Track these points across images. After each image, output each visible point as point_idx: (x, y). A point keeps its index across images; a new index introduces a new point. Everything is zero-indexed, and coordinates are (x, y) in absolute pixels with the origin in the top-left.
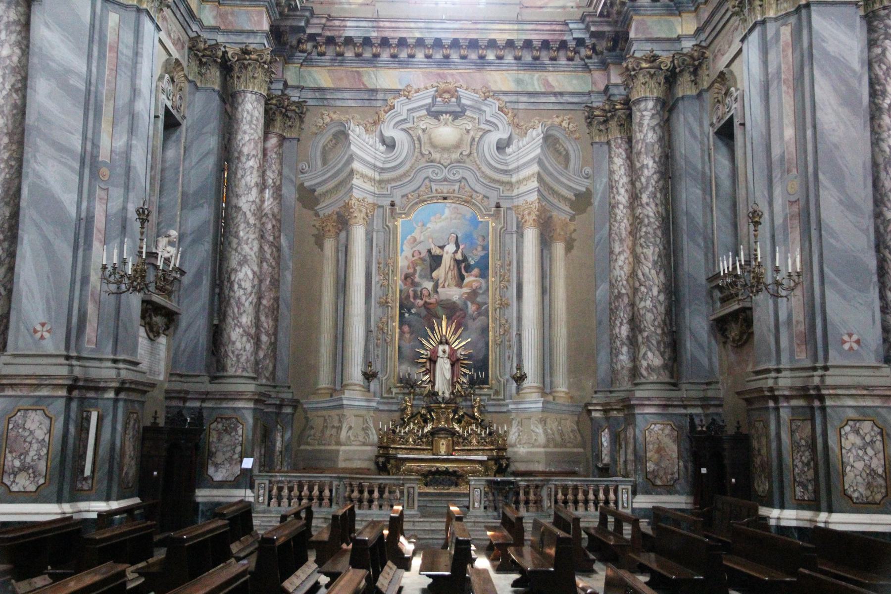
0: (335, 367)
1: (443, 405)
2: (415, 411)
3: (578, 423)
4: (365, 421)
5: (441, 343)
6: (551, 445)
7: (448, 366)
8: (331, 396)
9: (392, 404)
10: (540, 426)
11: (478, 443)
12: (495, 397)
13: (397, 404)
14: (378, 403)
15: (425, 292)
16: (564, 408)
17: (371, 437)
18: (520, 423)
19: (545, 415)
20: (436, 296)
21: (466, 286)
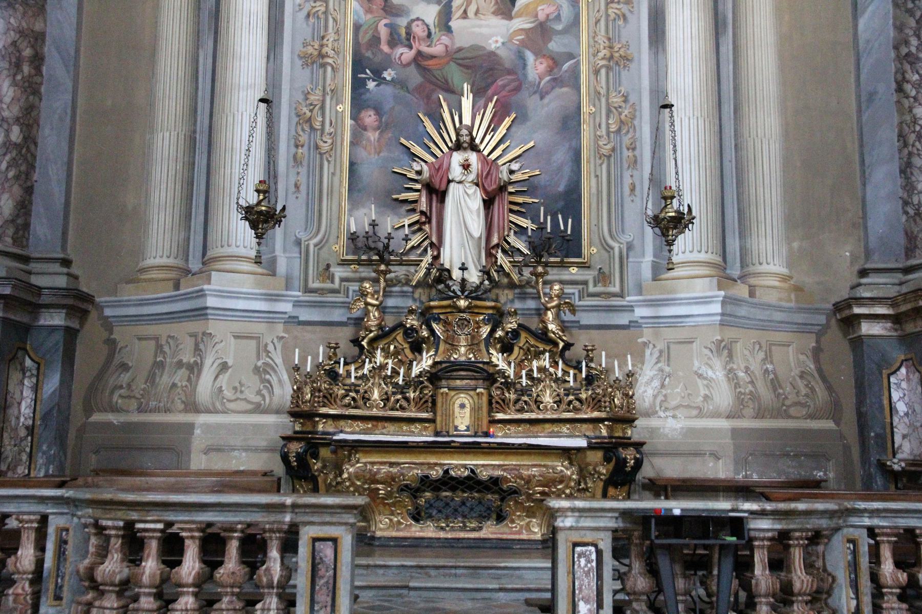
0: (187, 217)
1: (462, 303)
2: (390, 322)
3: (817, 353)
4: (262, 350)
5: (458, 146)
6: (749, 411)
7: (475, 201)
8: (177, 287)
9: (333, 305)
10: (718, 363)
11: (559, 402)
12: (600, 289)
13: (347, 306)
14: (297, 304)
15: (418, 30)
16: (778, 316)
17: (277, 390)
18: (666, 355)
19: (731, 333)
20: (445, 39)
21: (519, 15)
